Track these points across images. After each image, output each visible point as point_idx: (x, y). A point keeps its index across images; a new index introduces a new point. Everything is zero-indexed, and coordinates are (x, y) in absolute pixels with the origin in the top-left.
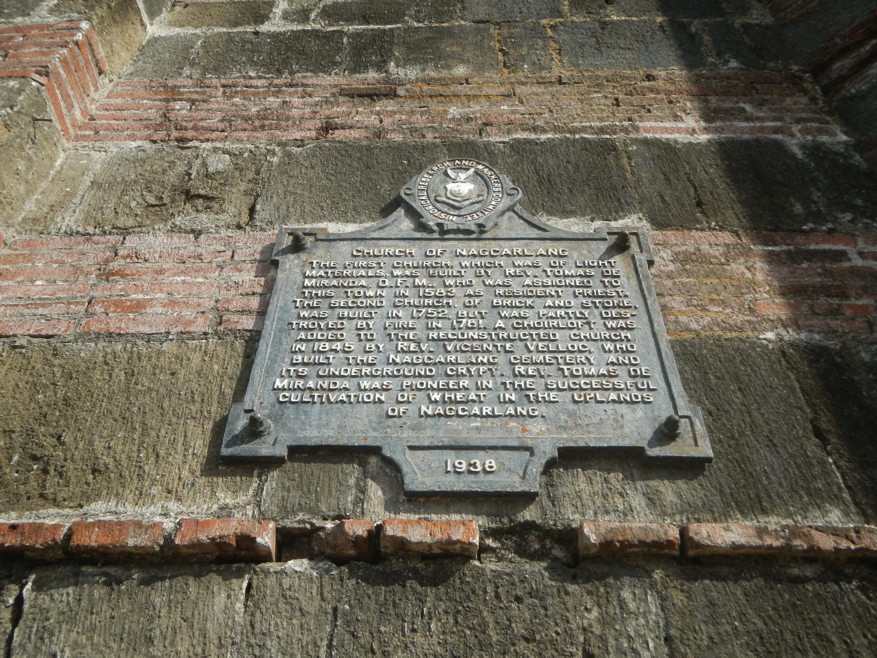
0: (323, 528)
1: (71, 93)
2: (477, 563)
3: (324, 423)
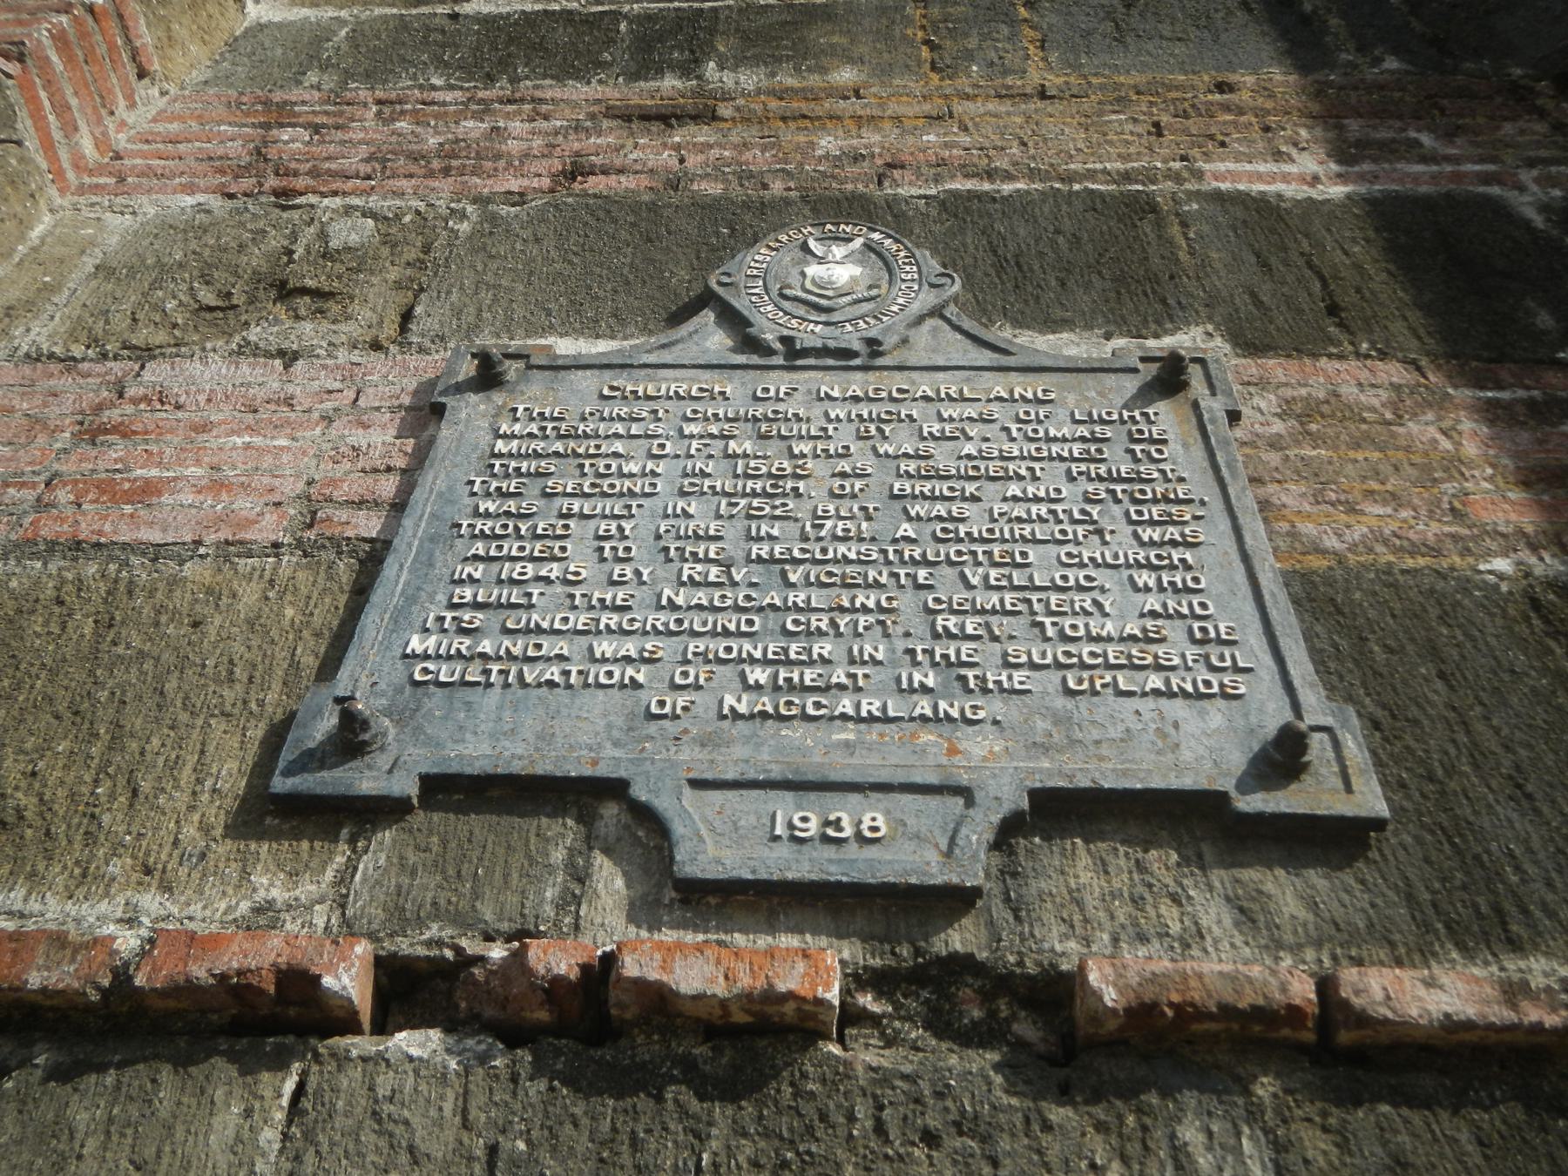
0: (481, 959)
1: (74, 102)
2: (835, 1049)
3: (507, 727)
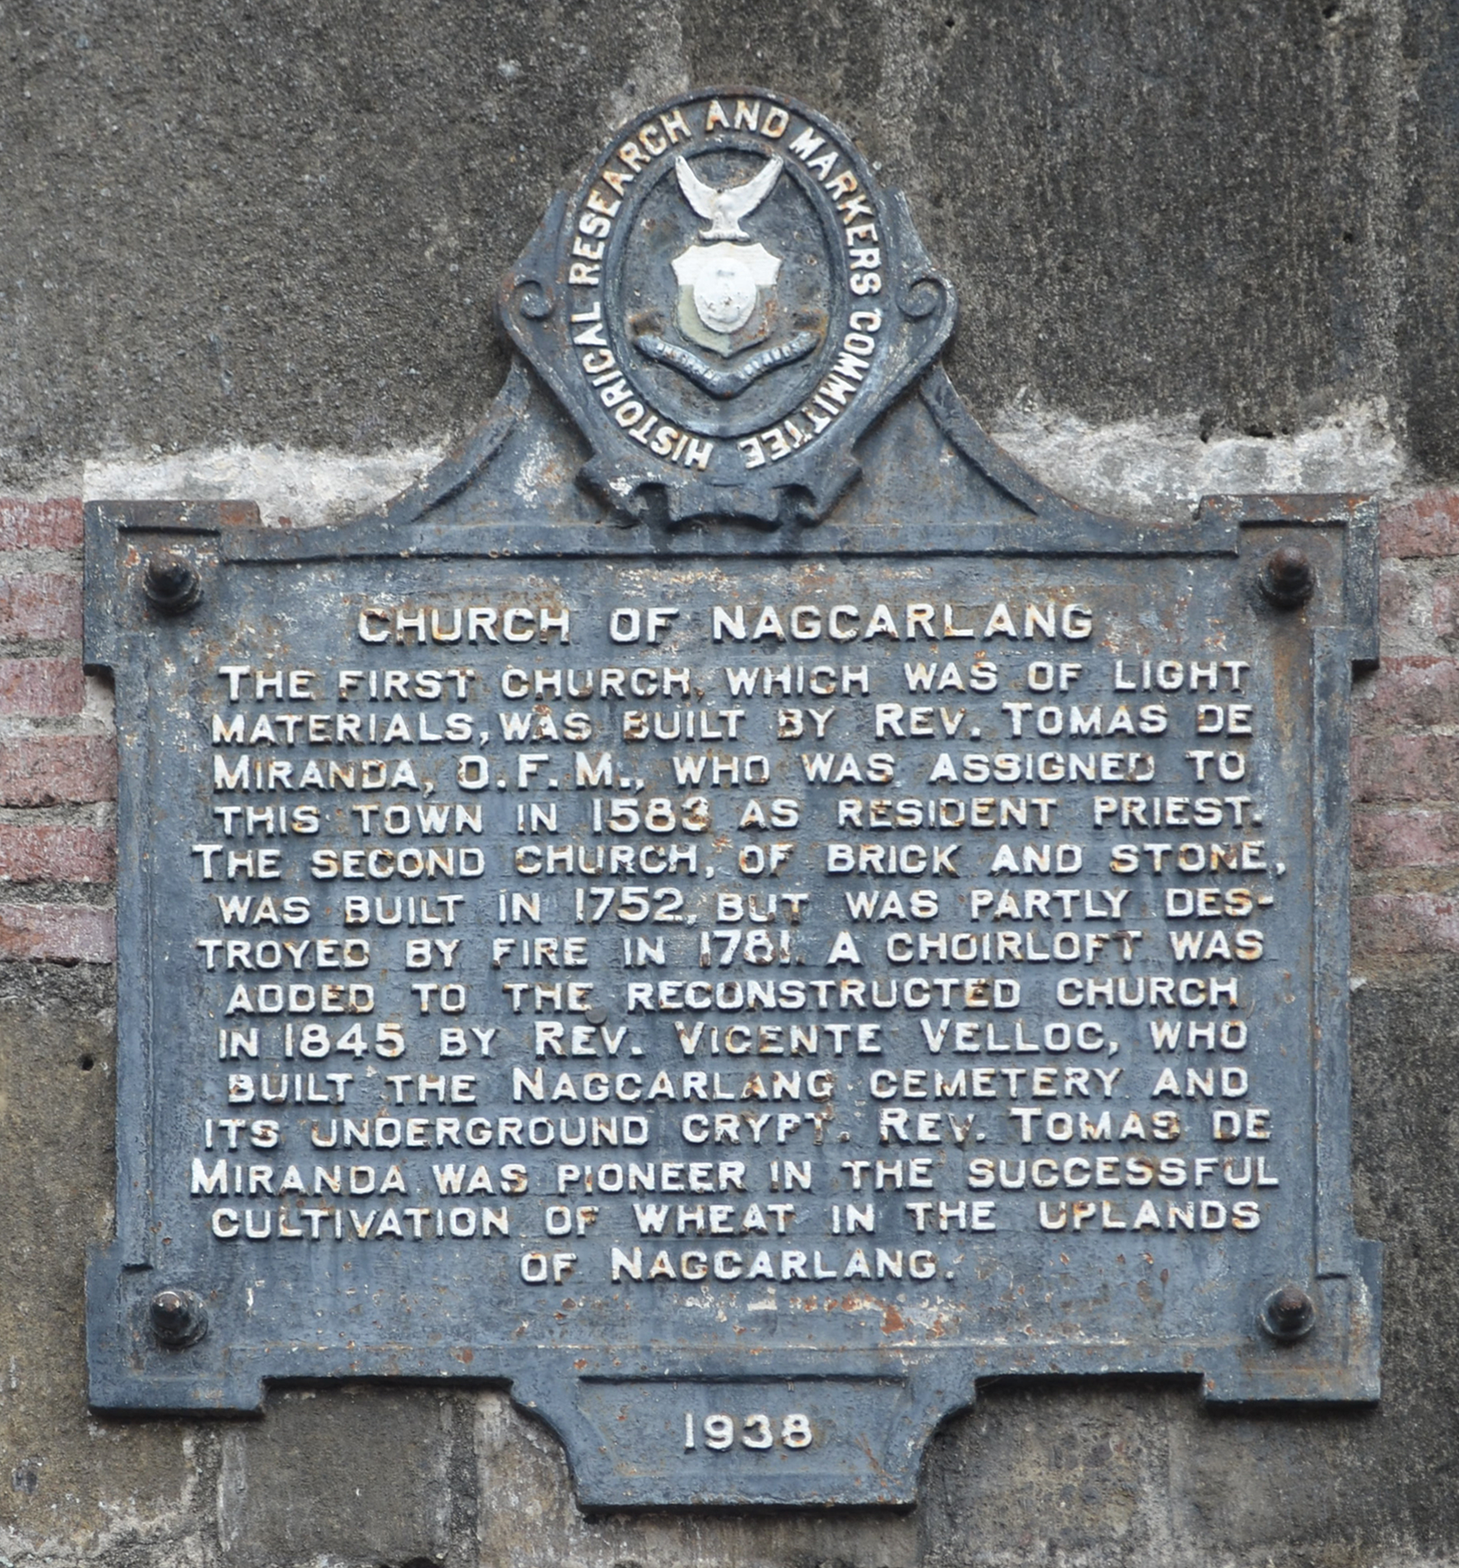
3: (349, 1304)
